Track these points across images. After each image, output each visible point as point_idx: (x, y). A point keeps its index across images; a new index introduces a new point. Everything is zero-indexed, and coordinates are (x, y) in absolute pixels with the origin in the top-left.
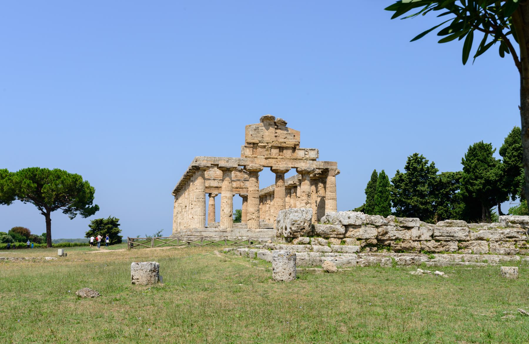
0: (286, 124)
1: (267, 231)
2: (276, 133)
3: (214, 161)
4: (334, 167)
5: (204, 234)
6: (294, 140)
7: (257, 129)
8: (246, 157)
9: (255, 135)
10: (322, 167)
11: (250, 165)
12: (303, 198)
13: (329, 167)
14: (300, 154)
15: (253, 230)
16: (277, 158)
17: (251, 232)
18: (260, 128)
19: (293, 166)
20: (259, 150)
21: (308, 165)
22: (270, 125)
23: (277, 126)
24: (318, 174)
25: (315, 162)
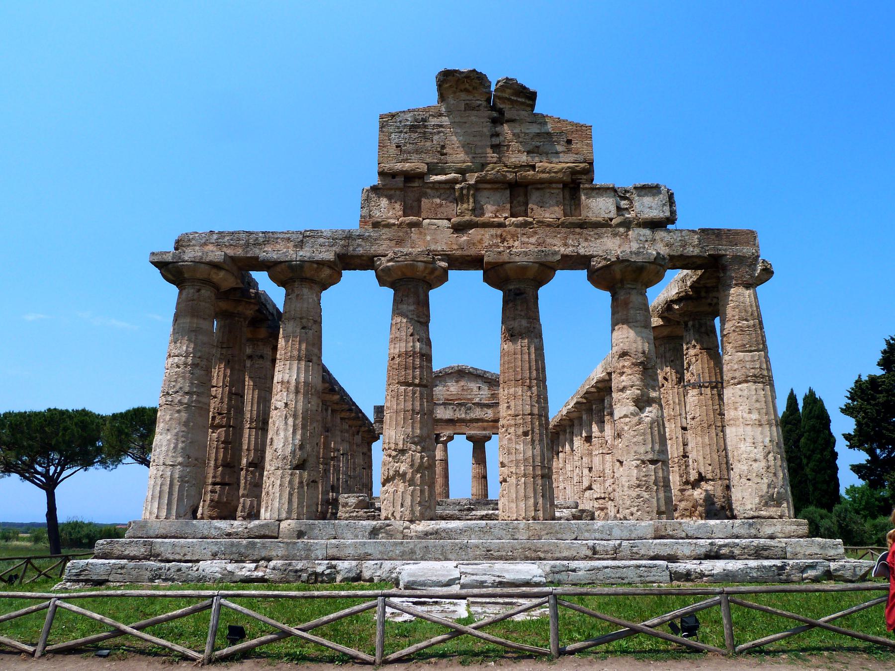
0: (532, 96)
1: (462, 532)
2: (497, 135)
3: (247, 245)
4: (747, 250)
5: (164, 546)
6: (571, 157)
7: (418, 125)
8: (376, 225)
9: (409, 147)
10: (697, 251)
11: (391, 255)
12: (625, 380)
13: (728, 251)
14: (600, 207)
15: (398, 524)
16: (500, 225)
17: (390, 535)
19: (568, 251)
21: (635, 246)
22: (469, 107)
23: (501, 112)
24: (678, 300)
25: (660, 234)
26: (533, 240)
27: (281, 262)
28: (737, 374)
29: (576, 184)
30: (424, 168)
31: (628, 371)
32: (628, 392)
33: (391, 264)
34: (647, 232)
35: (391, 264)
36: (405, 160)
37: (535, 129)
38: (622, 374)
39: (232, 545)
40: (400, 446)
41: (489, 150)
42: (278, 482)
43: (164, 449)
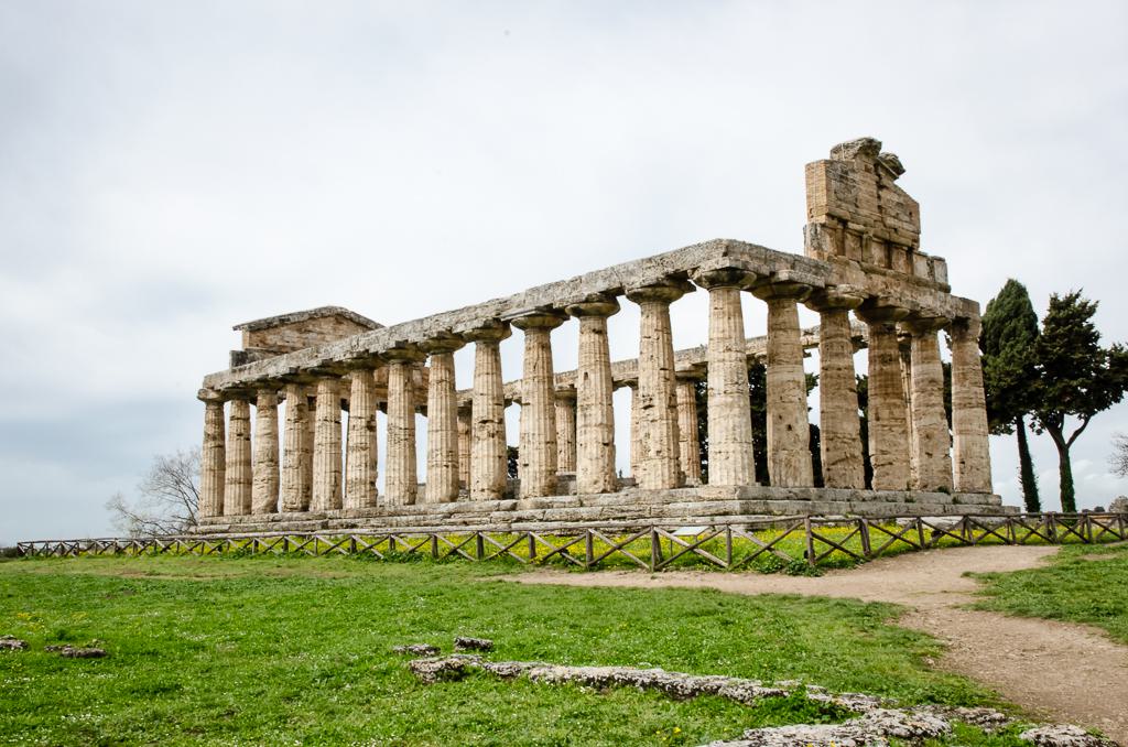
9: (841, 196)
16: (884, 274)
18: (851, 176)
20: (850, 242)
21: (939, 304)
22: (867, 170)
26: (899, 290)
27: (796, 283)
28: (974, 401)
29: (911, 251)
30: (848, 217)
31: (937, 394)
32: (937, 408)
33: (846, 296)
34: (942, 294)
35: (846, 296)
36: (839, 206)
37: (896, 199)
38: (931, 394)
39: (806, 505)
40: (854, 437)
41: (877, 210)
42: (803, 460)
43: (744, 429)
